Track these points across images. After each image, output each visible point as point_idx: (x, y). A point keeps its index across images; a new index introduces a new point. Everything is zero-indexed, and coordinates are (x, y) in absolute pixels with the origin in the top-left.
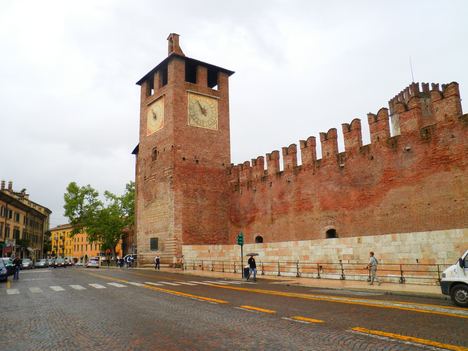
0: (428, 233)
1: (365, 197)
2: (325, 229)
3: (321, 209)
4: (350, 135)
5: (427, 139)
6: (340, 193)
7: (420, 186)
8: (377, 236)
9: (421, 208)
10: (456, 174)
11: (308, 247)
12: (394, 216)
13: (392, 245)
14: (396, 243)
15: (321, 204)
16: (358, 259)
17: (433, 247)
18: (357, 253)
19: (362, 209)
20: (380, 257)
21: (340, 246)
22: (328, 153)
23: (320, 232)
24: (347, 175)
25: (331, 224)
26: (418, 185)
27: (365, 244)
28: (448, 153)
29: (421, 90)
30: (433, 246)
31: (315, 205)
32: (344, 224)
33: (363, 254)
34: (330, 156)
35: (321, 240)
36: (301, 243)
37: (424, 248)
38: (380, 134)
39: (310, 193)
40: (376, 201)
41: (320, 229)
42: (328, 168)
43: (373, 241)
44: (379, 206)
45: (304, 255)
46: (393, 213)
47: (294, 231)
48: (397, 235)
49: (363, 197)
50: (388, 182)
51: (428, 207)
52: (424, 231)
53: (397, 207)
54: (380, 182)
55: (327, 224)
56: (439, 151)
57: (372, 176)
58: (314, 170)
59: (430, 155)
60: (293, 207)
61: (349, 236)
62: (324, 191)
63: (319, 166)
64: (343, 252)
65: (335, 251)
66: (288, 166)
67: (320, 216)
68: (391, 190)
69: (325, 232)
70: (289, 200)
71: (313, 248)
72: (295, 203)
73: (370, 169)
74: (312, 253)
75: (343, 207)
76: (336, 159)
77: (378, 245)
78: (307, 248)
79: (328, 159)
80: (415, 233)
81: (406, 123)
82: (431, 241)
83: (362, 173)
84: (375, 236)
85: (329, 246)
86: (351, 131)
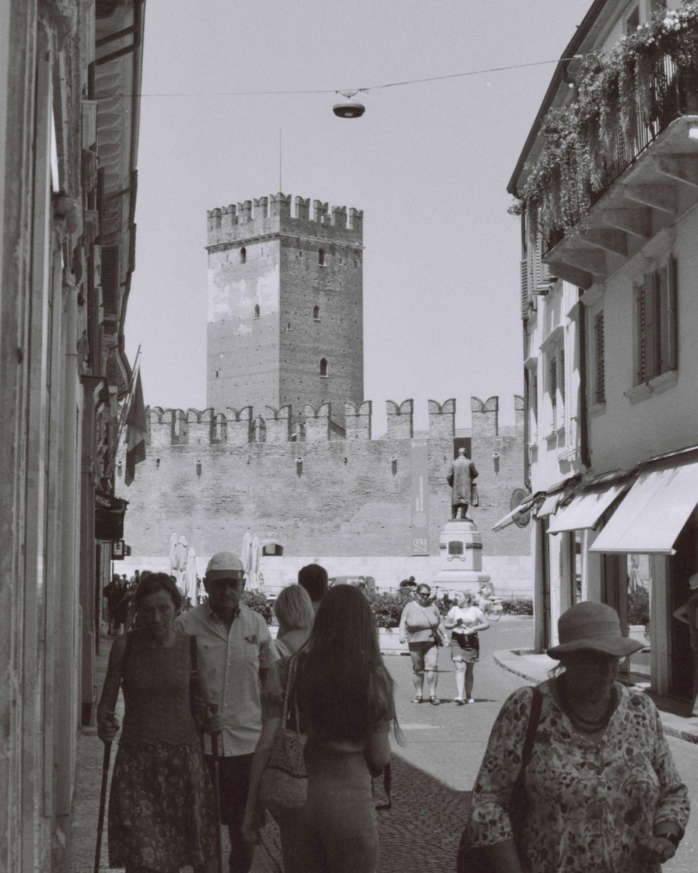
3: (258, 513)
4: (316, 422)
7: (403, 505)
8: (342, 558)
25: (273, 537)
29: (294, 214)
39: (239, 489)
48: (370, 559)
53: (372, 526)
54: (353, 492)
55: (267, 537)
58: (250, 457)
61: (300, 555)
66: (199, 440)
68: (367, 504)
70: (195, 493)
81: (395, 428)
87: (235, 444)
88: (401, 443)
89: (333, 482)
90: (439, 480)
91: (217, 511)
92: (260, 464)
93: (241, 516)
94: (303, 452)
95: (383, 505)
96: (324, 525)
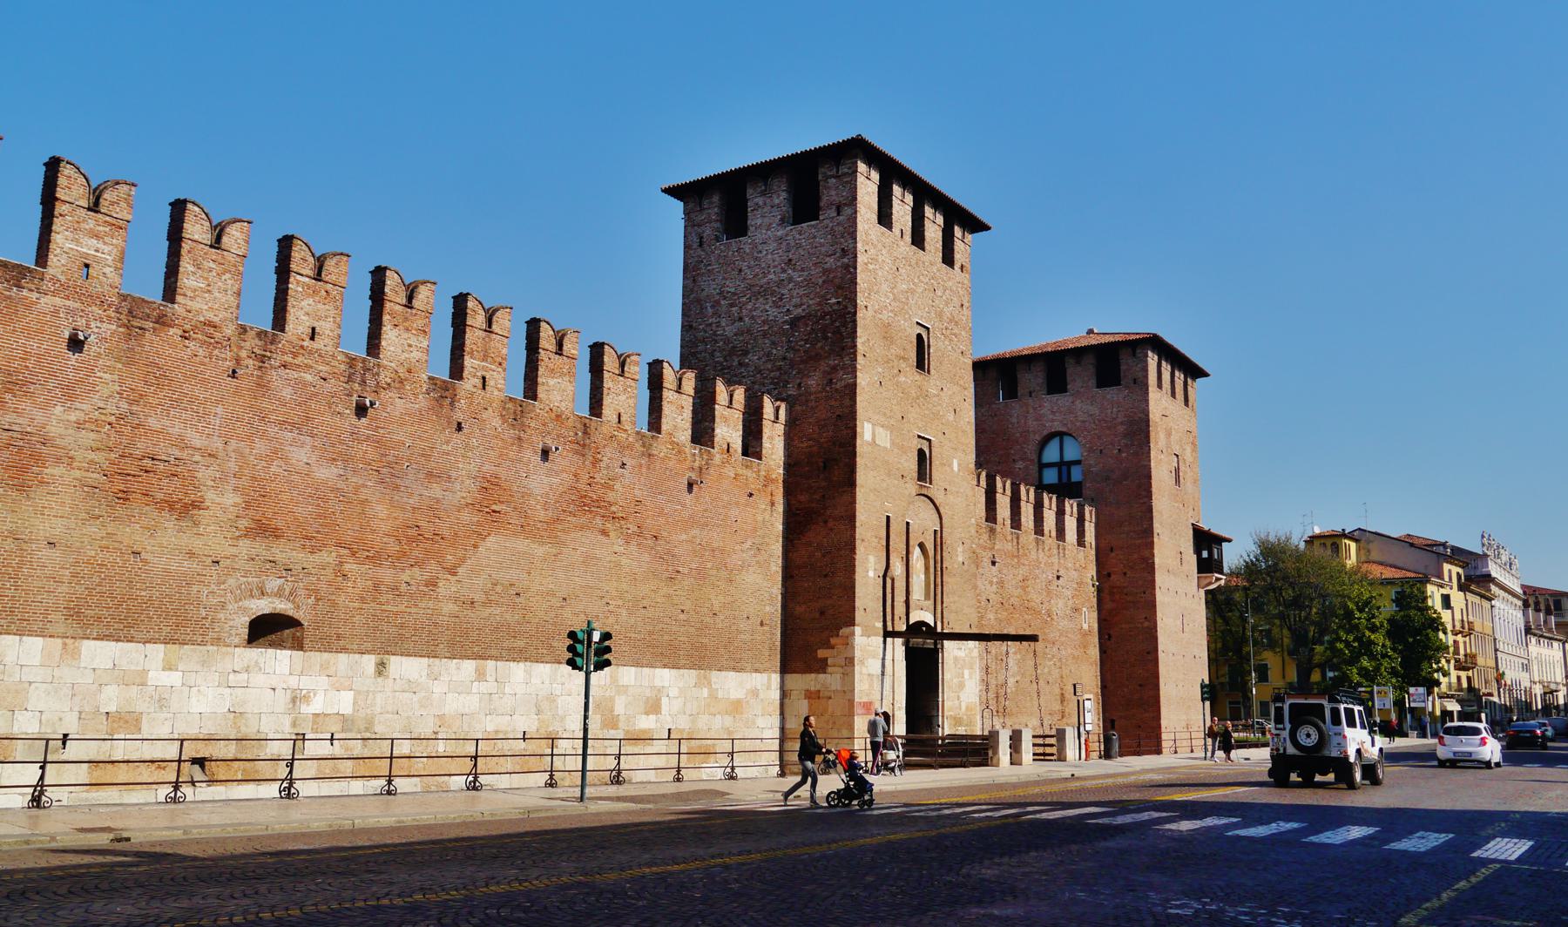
0: (553, 668)
1: (419, 535)
2: (245, 610)
3: (243, 523)
4: (406, 319)
5: (584, 446)
6: (335, 490)
7: (554, 551)
8: (437, 661)
9: (548, 603)
10: (616, 548)
11: (145, 672)
12: (489, 611)
13: (474, 691)
14: (483, 687)
15: (248, 505)
16: (367, 729)
17: (559, 702)
18: (369, 711)
19: (403, 570)
20: (439, 724)
21: (306, 683)
22: (313, 329)
23: (221, 616)
24: (374, 441)
25: (279, 594)
26: (550, 545)
27: (398, 680)
28: (611, 496)
30: (559, 701)
31: (218, 500)
32: (334, 604)
33: (388, 712)
34: (318, 344)
35: (224, 649)
36: (99, 653)
37: (541, 704)
38: (491, 372)
39: (198, 443)
40: (449, 557)
41: (223, 605)
42: (305, 384)
43: (424, 673)
44: (454, 574)
45: (112, 708)
46: (488, 603)
47: (64, 588)
48: (490, 664)
49: (412, 532)
50: (487, 512)
51: (562, 607)
52: (547, 662)
53: (499, 589)
54: (467, 505)
56: (596, 483)
57: (449, 477)
58: (238, 360)
59: (582, 486)
60: (78, 474)
61: (344, 650)
62: (269, 459)
63: (264, 356)
64: (316, 706)
65: (282, 699)
67: (234, 550)
69: (248, 619)
70: (54, 429)
71: (174, 678)
72: (92, 456)
73: (448, 454)
74: (162, 703)
75: (339, 545)
76: (343, 367)
77: (438, 688)
78: (141, 679)
79: (310, 353)
80: (528, 664)
82: (557, 689)
83: (423, 455)
84: (432, 660)
85: (258, 679)
86: (411, 308)
87: (199, 312)
88: (558, 416)
89: (430, 475)
90: (613, 509)
91: (124, 497)
92: (262, 386)
93: (196, 524)
94: (371, 382)
95: (522, 544)
96: (405, 577)
